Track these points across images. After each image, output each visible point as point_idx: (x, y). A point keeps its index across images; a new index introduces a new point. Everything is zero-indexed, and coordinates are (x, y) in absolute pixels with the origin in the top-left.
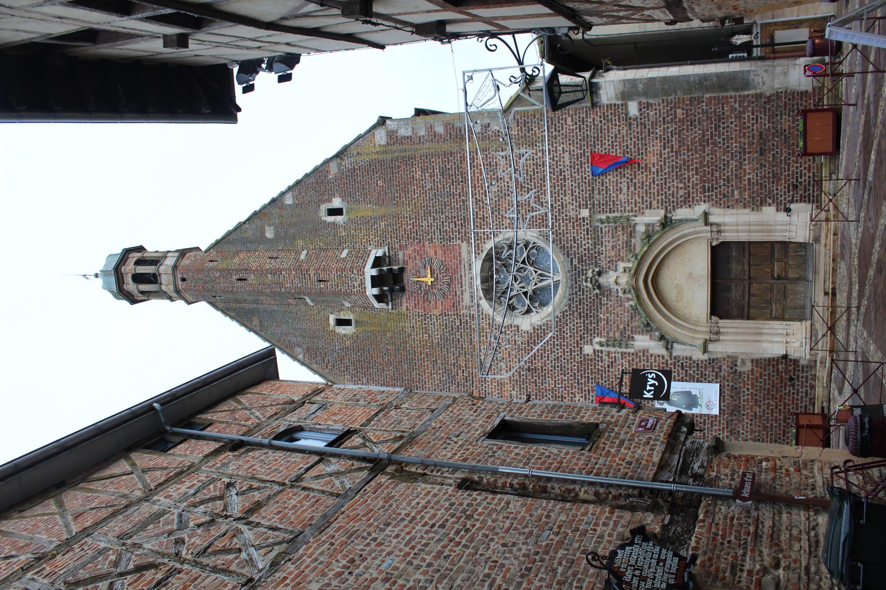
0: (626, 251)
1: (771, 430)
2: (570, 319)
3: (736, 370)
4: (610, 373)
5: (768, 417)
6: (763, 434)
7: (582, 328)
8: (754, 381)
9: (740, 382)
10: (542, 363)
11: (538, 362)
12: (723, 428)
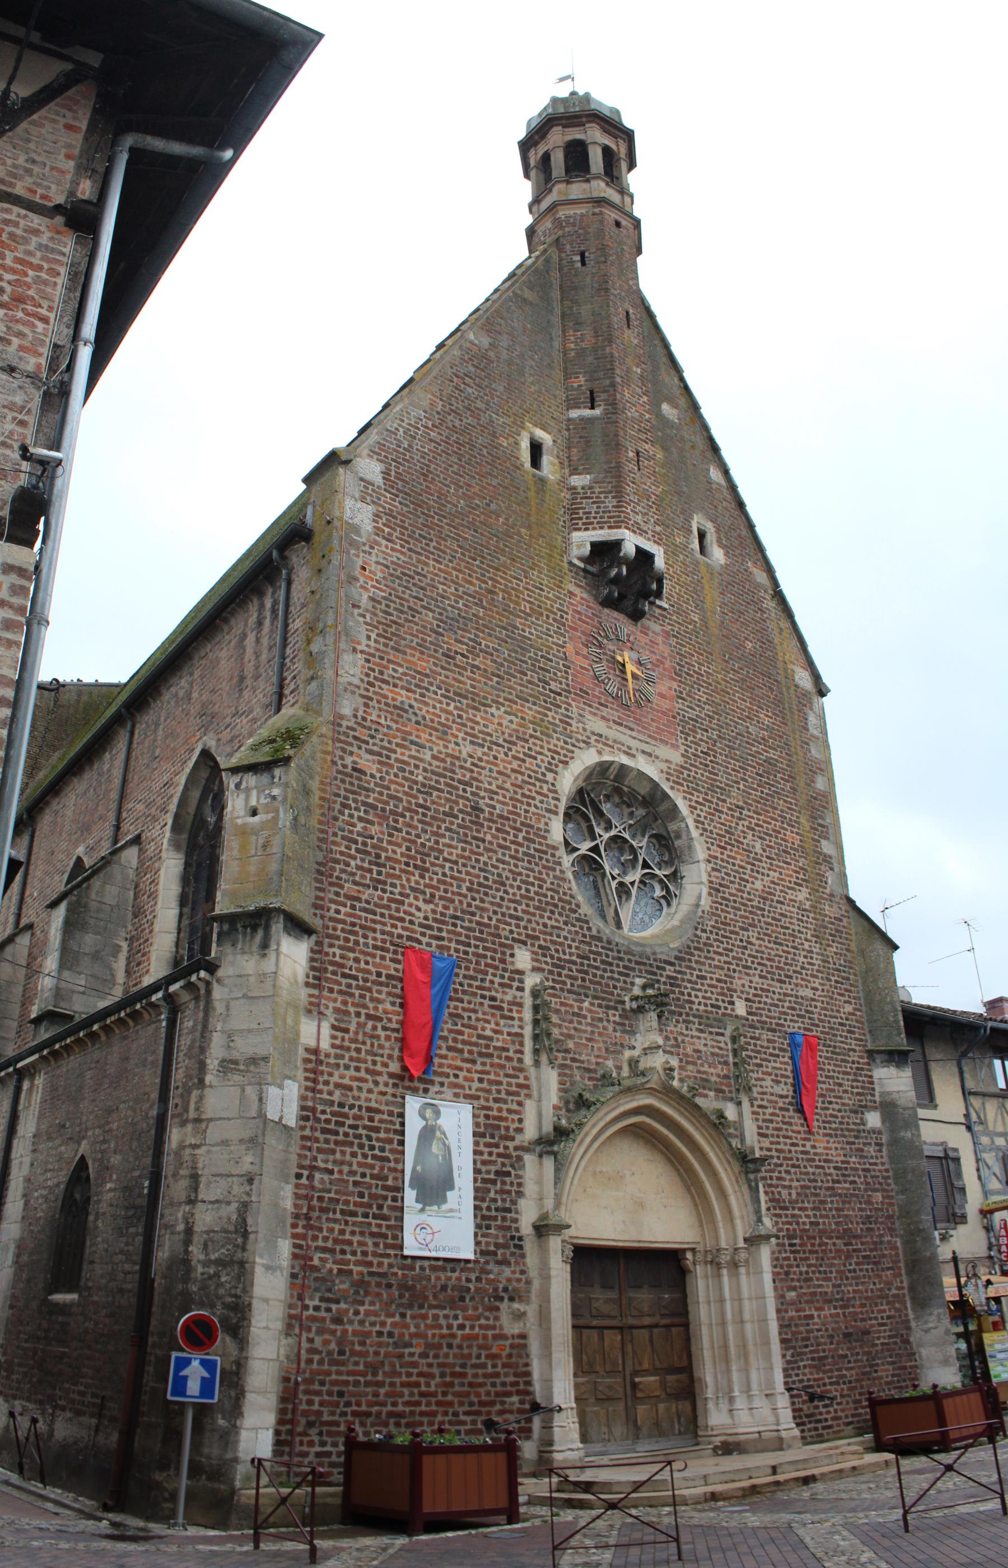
0: (696, 1078)
1: (367, 1384)
2: (577, 933)
3: (502, 1299)
4: (479, 1000)
5: (400, 1374)
6: (356, 1364)
7: (562, 956)
8: (481, 1341)
9: (476, 1308)
10: (491, 843)
11: (493, 836)
12: (370, 1264)
